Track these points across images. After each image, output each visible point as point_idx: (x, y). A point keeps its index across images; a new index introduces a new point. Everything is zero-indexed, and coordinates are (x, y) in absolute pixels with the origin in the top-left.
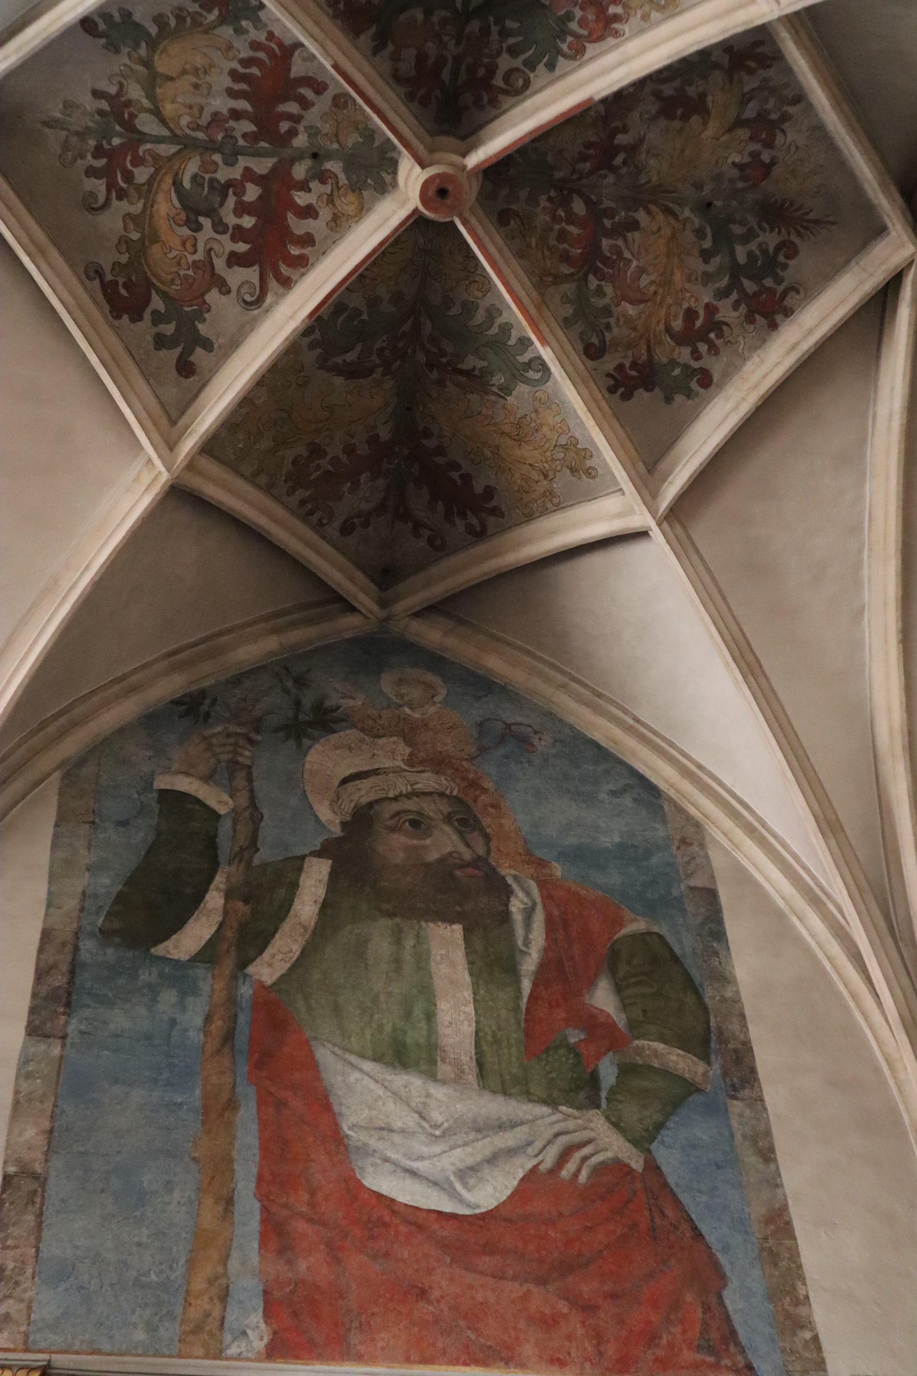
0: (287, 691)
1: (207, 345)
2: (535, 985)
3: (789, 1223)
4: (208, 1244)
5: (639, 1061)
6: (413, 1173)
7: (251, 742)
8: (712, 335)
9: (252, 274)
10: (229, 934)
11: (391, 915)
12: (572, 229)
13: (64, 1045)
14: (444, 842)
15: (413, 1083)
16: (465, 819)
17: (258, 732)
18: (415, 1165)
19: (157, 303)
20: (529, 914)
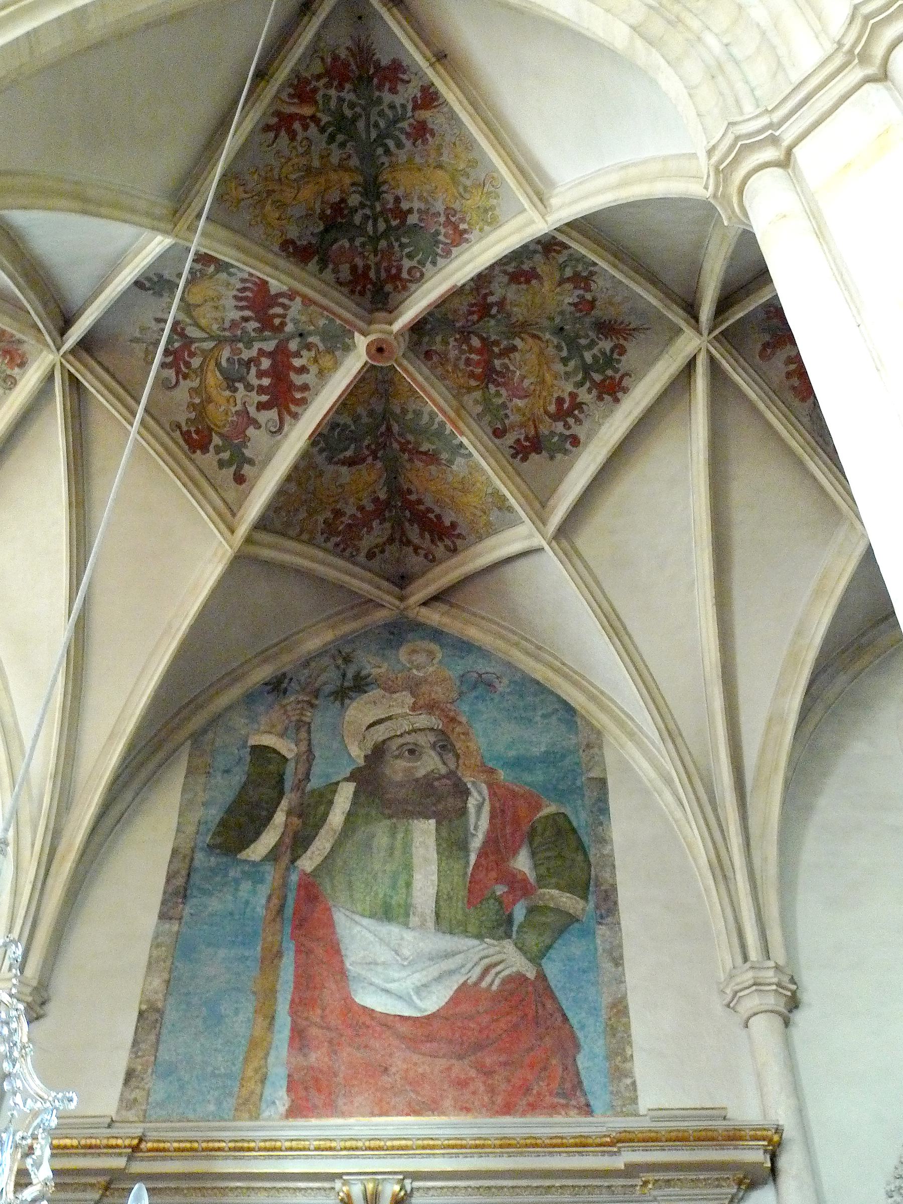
0: (338, 667)
1: (251, 462)
2: (479, 856)
3: (626, 1007)
4: (258, 1046)
5: (541, 903)
6: (387, 991)
7: (312, 706)
8: (576, 412)
9: (273, 414)
10: (287, 840)
11: (390, 817)
12: (473, 356)
13: (180, 923)
14: (430, 763)
15: (393, 931)
17: (316, 697)
18: (389, 986)
19: (216, 440)
20: (479, 808)
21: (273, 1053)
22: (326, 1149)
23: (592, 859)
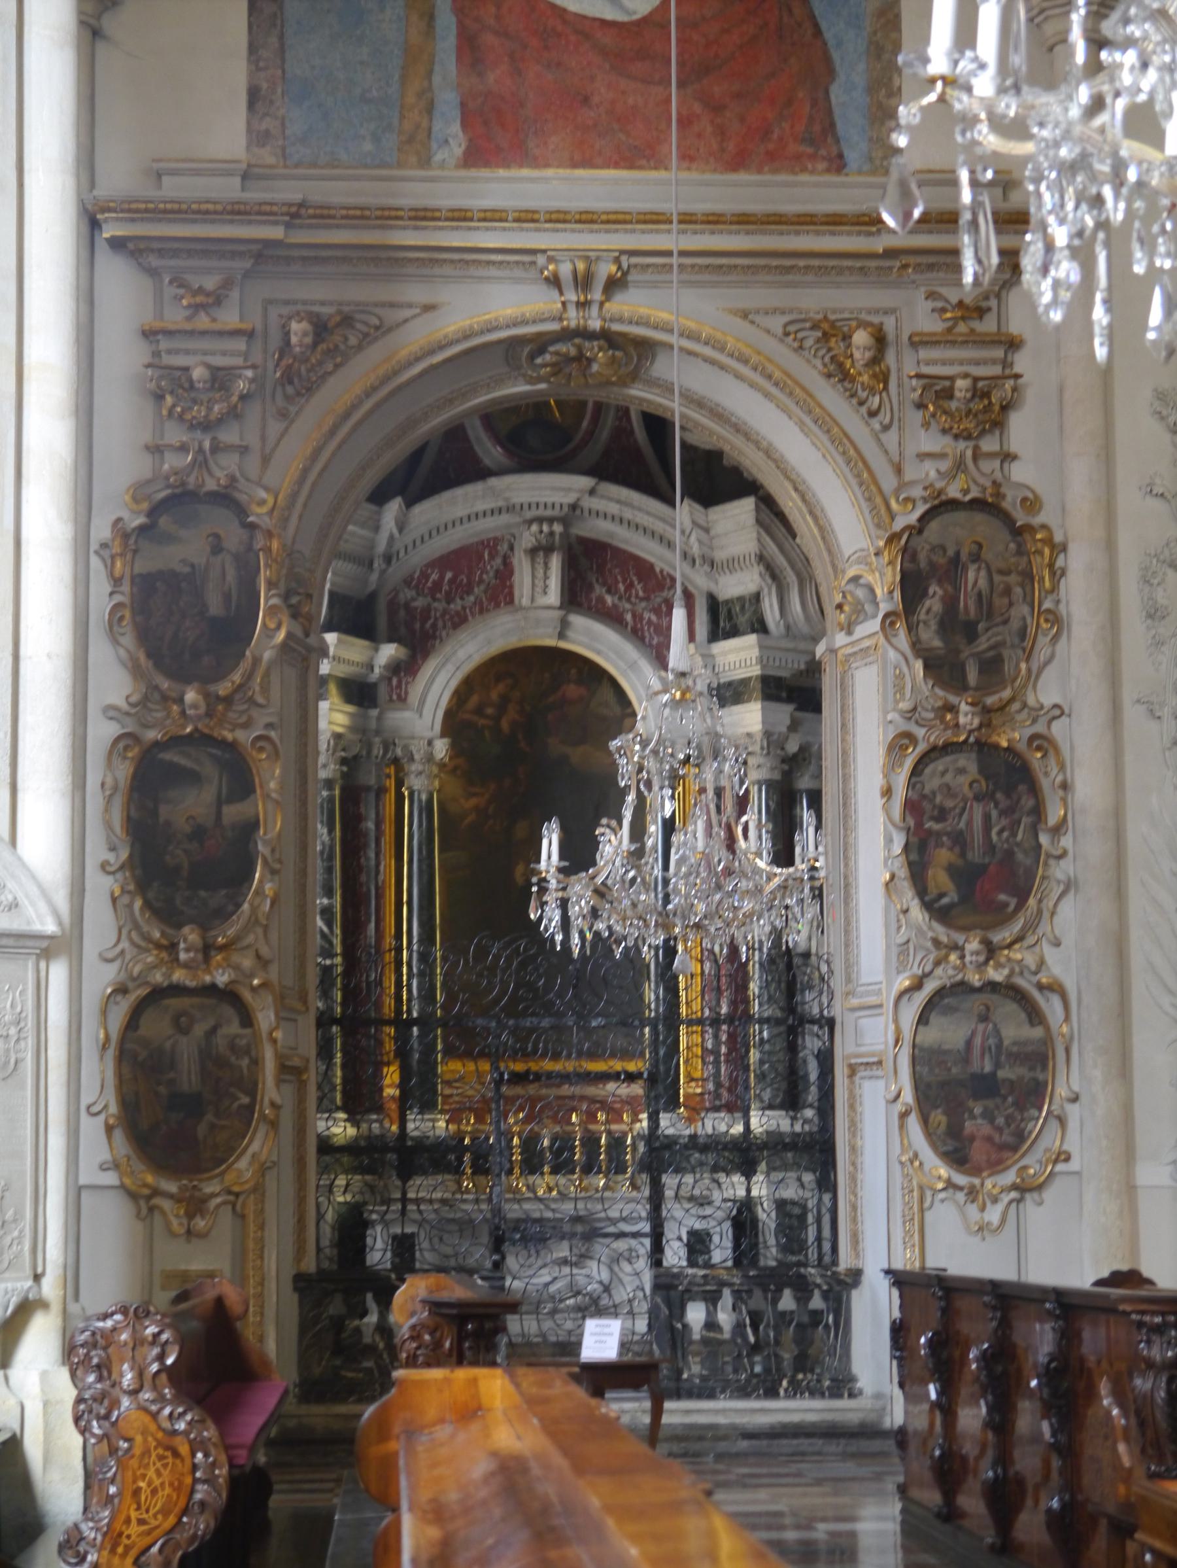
3: (898, 16)
4: (417, 59)
21: (437, 68)
22: (527, 218)
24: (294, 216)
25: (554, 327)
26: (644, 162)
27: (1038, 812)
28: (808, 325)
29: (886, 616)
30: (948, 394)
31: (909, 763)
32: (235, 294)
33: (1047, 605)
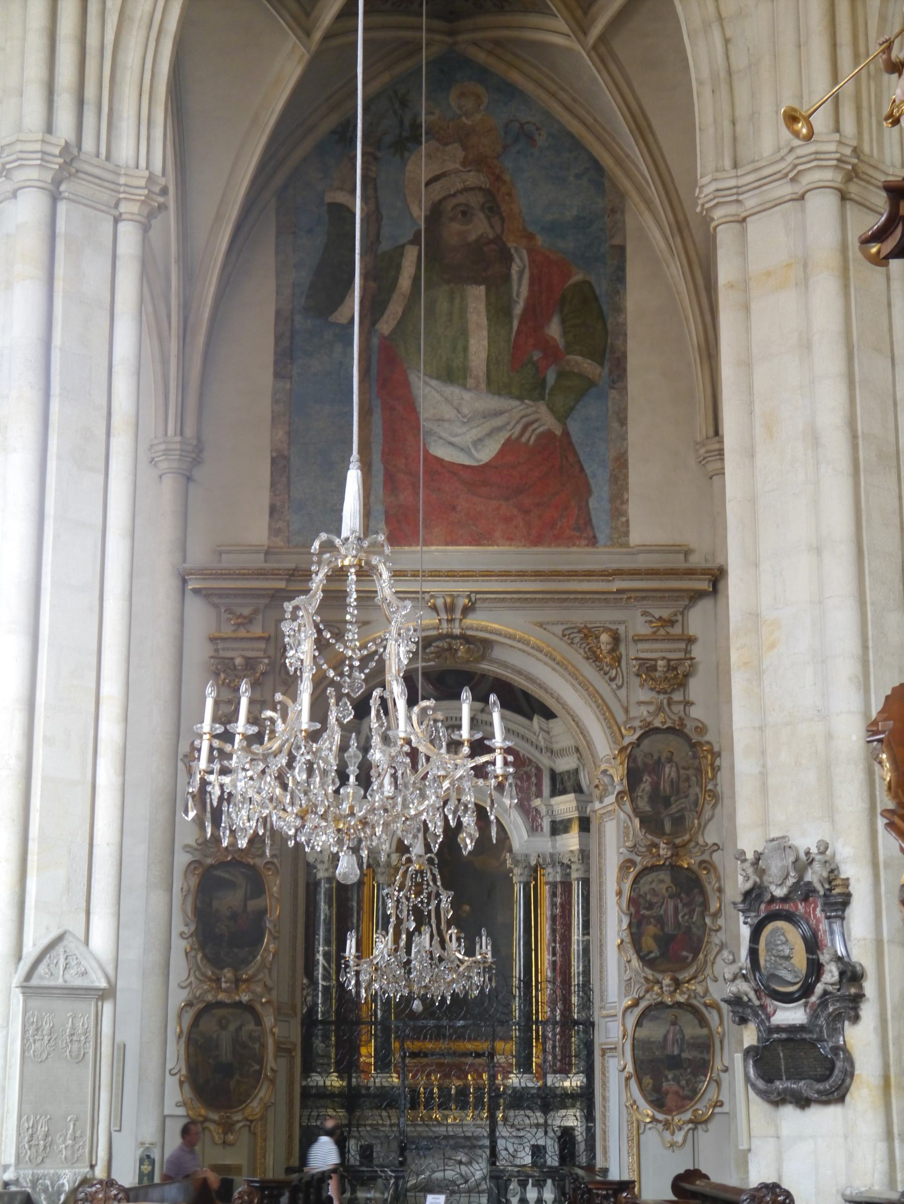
0: (395, 112)
2: (520, 323)
3: (626, 461)
5: (568, 369)
6: (452, 444)
7: (376, 159)
13: (291, 382)
14: (480, 227)
16: (492, 208)
18: (453, 440)
20: (521, 273)
23: (609, 327)
24: (292, 575)
25: (434, 633)
26: (486, 542)
27: (705, 905)
28: (576, 630)
29: (619, 793)
30: (654, 668)
31: (631, 877)
32: (260, 617)
33: (710, 787)
